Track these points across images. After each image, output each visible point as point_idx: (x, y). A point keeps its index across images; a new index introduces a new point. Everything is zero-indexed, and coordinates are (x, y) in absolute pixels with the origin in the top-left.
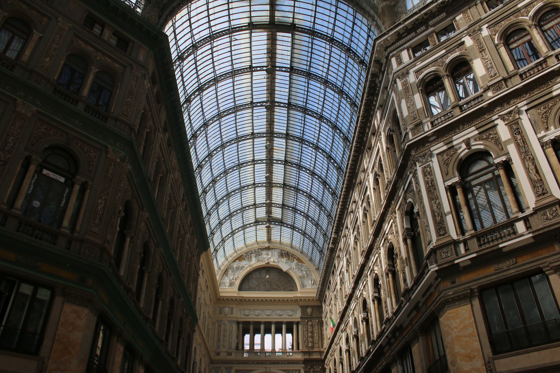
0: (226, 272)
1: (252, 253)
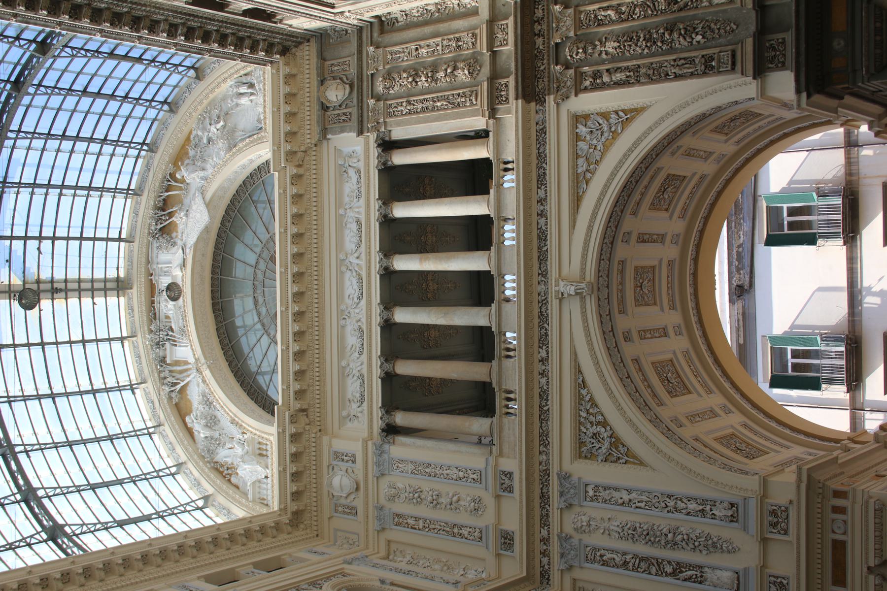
0: (224, 473)
1: (163, 360)
